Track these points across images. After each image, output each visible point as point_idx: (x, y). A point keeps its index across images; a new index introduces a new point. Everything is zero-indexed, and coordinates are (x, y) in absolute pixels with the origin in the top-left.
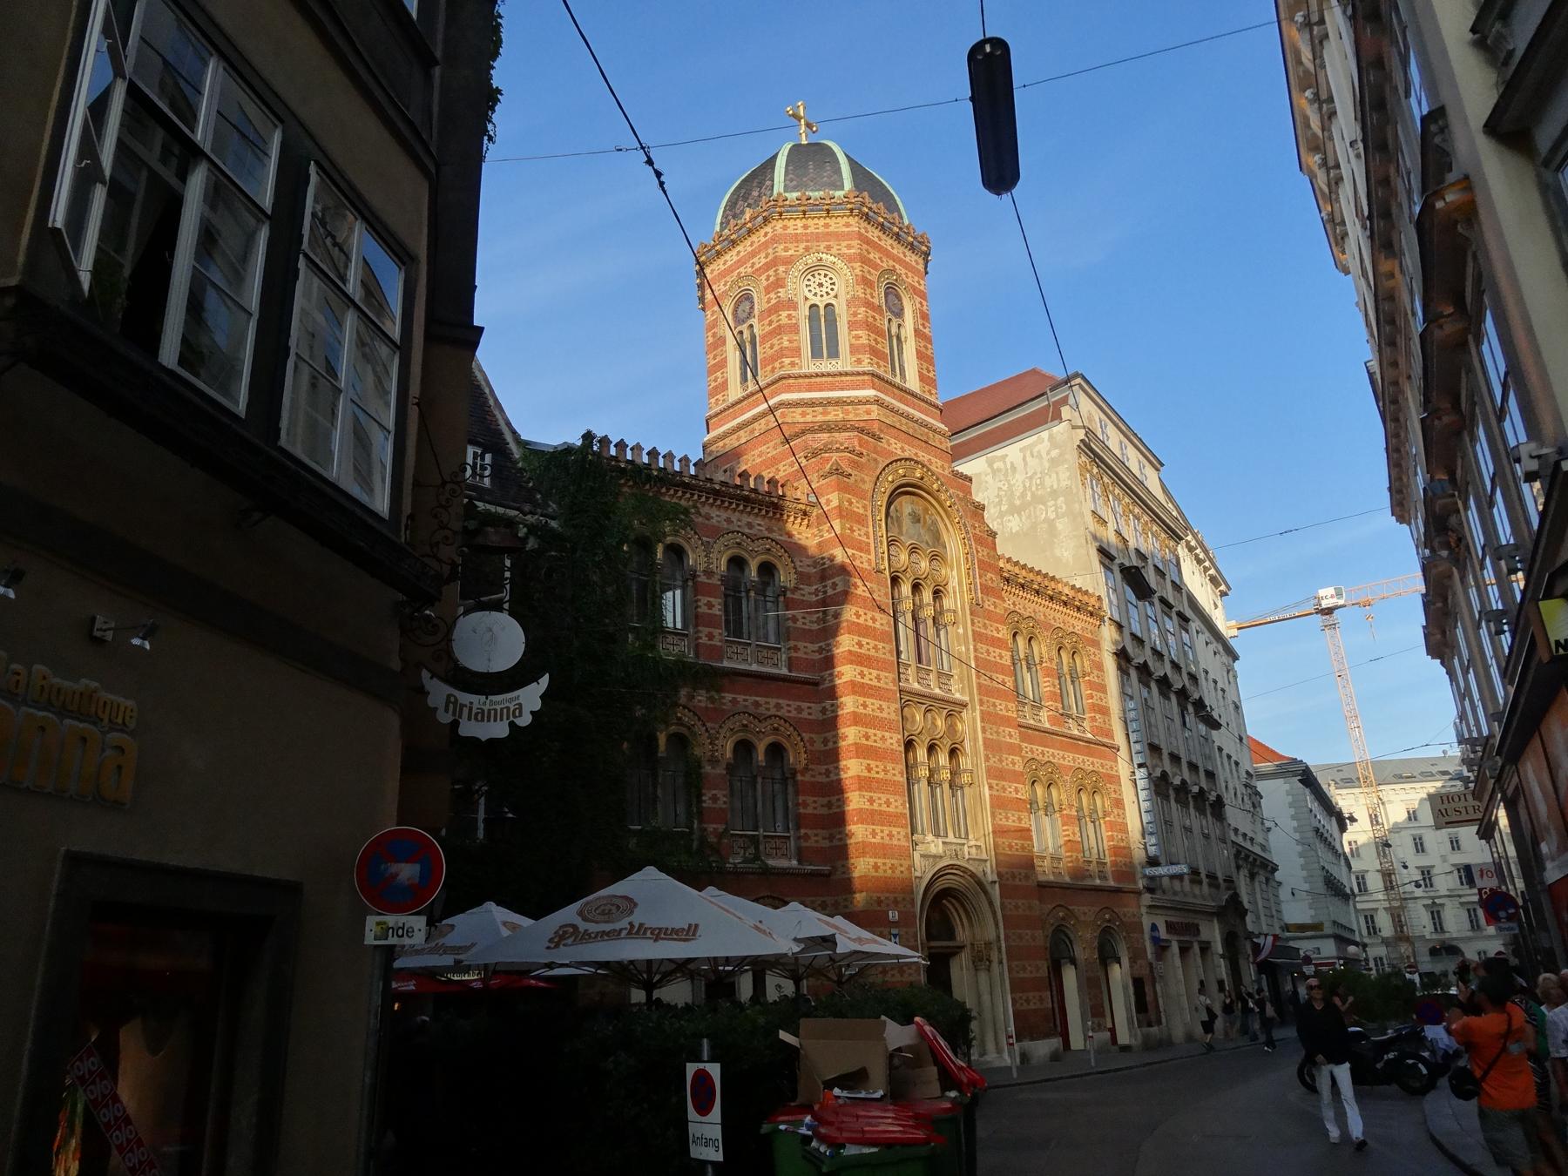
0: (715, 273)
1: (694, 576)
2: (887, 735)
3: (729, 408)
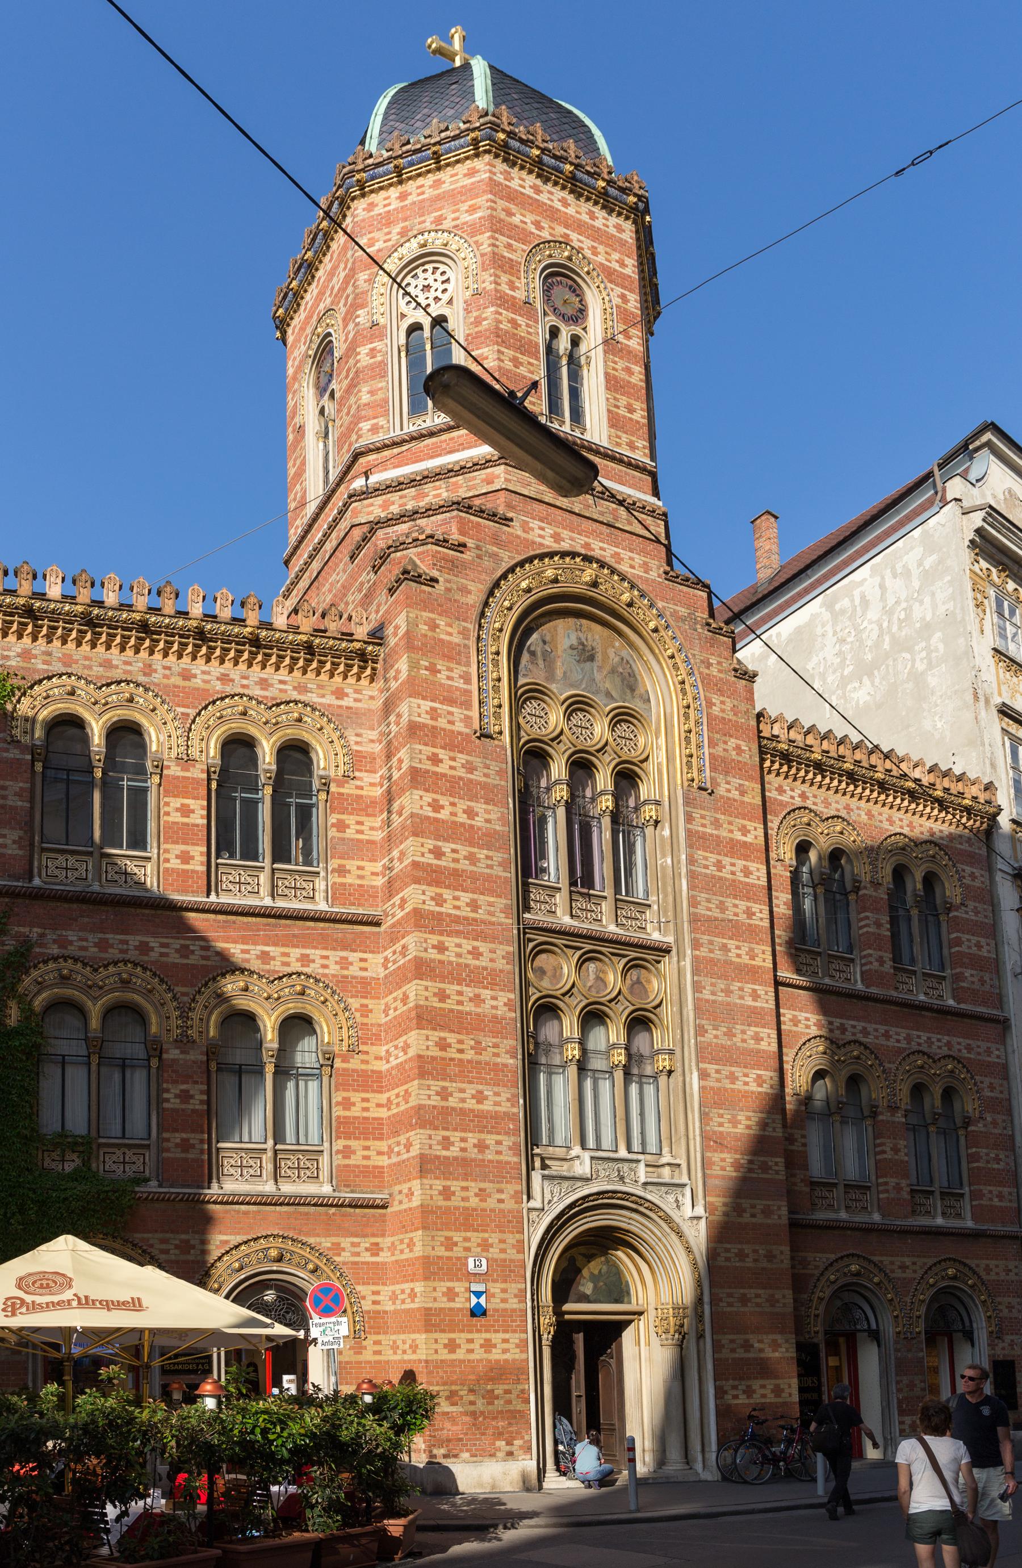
2: (486, 994)
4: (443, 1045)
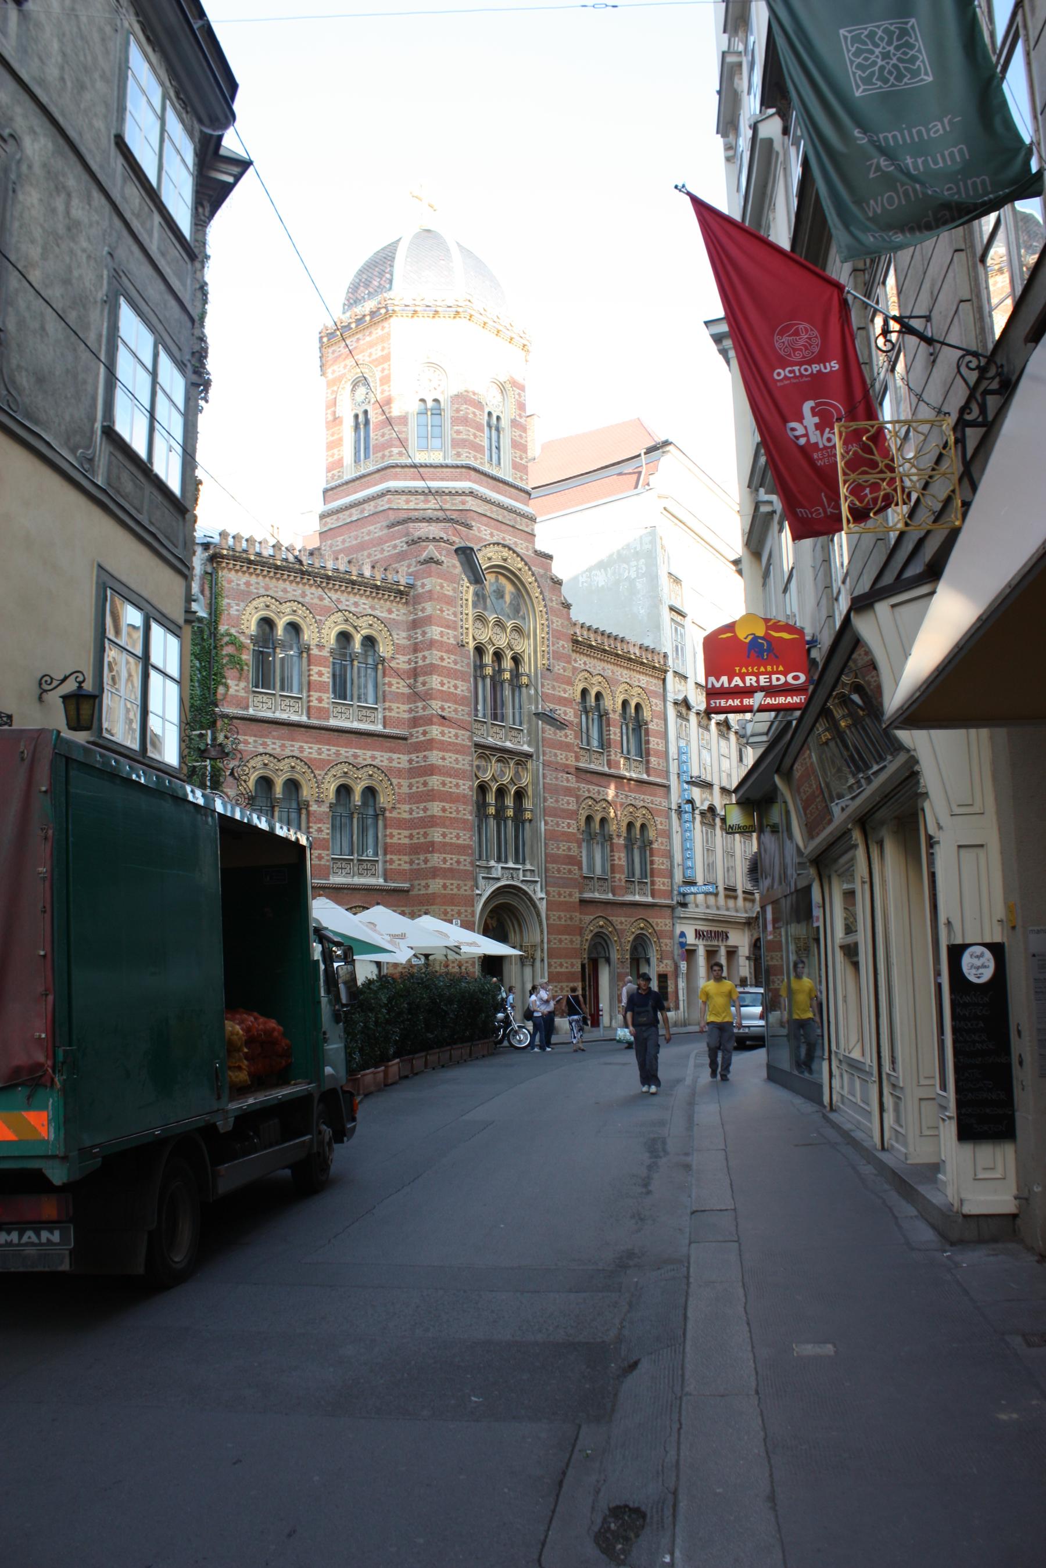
1: (308, 649)
2: (461, 782)
3: (343, 484)
4: (444, 810)
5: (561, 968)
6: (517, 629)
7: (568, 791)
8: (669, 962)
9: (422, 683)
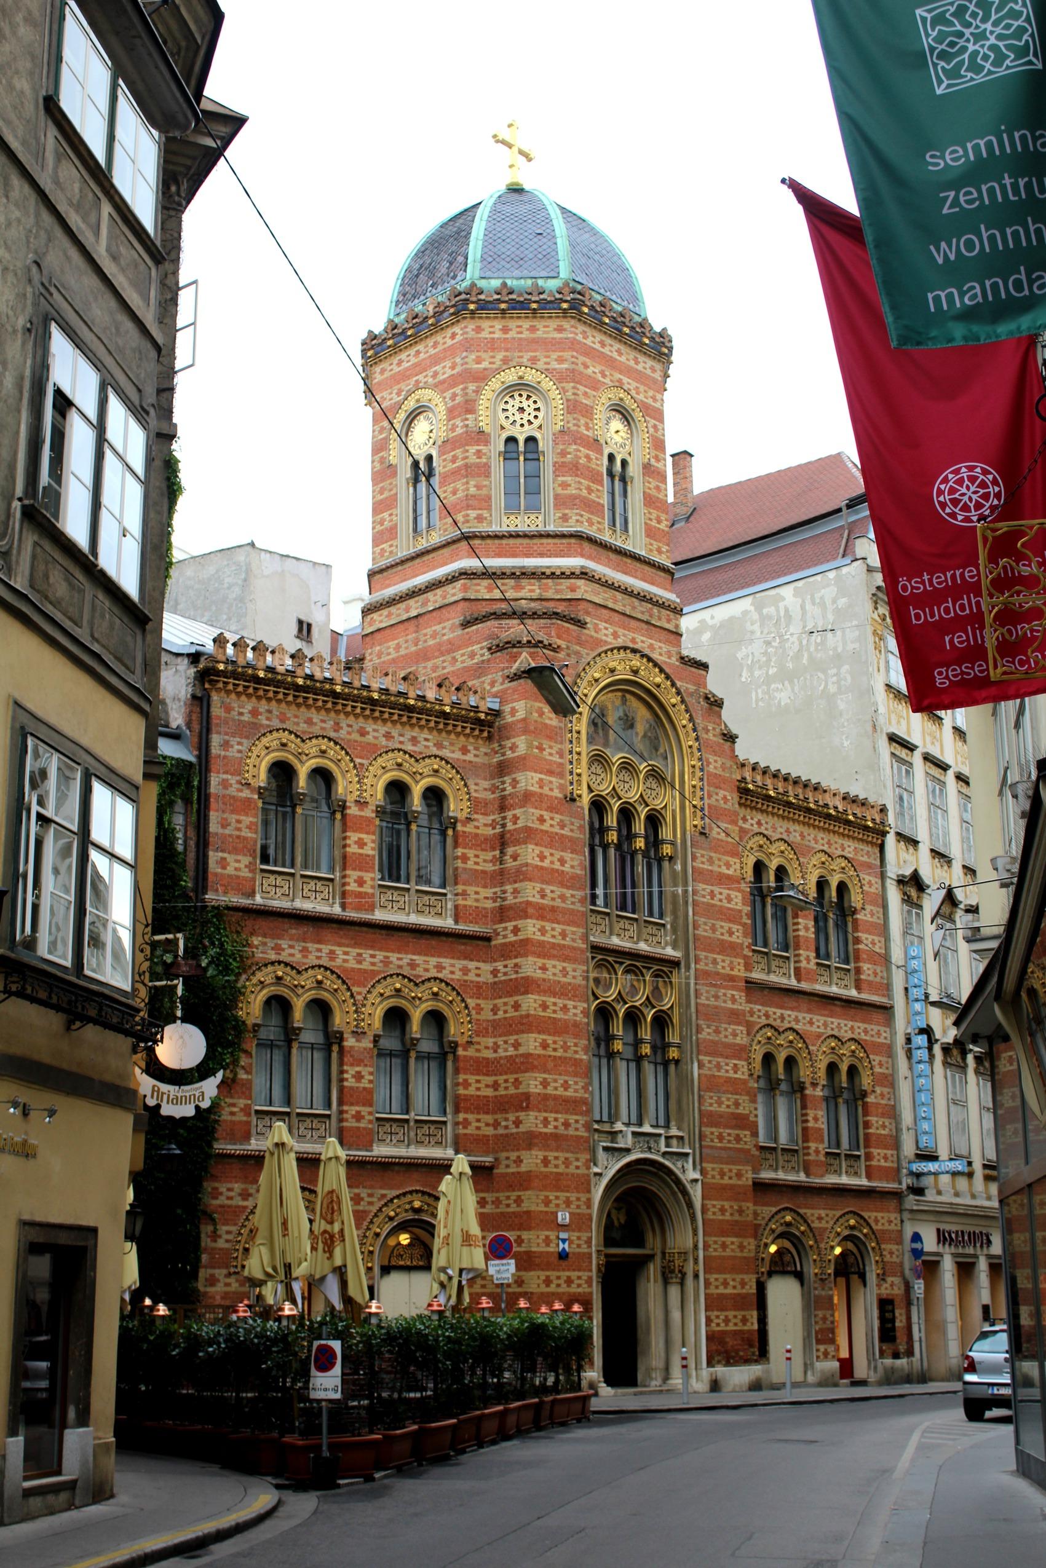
0: (387, 374)
1: (343, 807)
2: (570, 1004)
3: (397, 564)
4: (545, 1046)
5: (725, 1288)
6: (655, 775)
7: (735, 1016)
8: (897, 1280)
9: (511, 857)
